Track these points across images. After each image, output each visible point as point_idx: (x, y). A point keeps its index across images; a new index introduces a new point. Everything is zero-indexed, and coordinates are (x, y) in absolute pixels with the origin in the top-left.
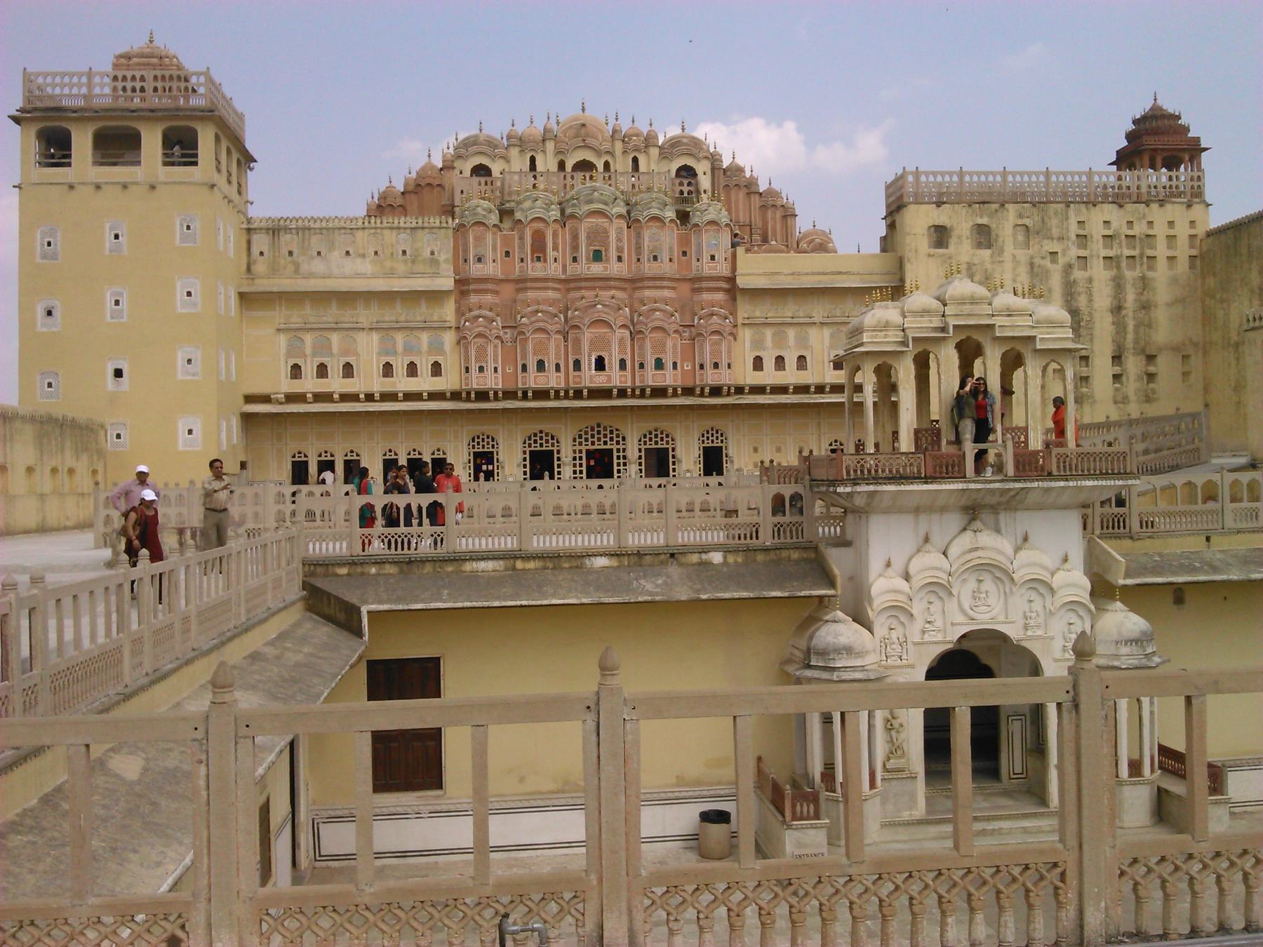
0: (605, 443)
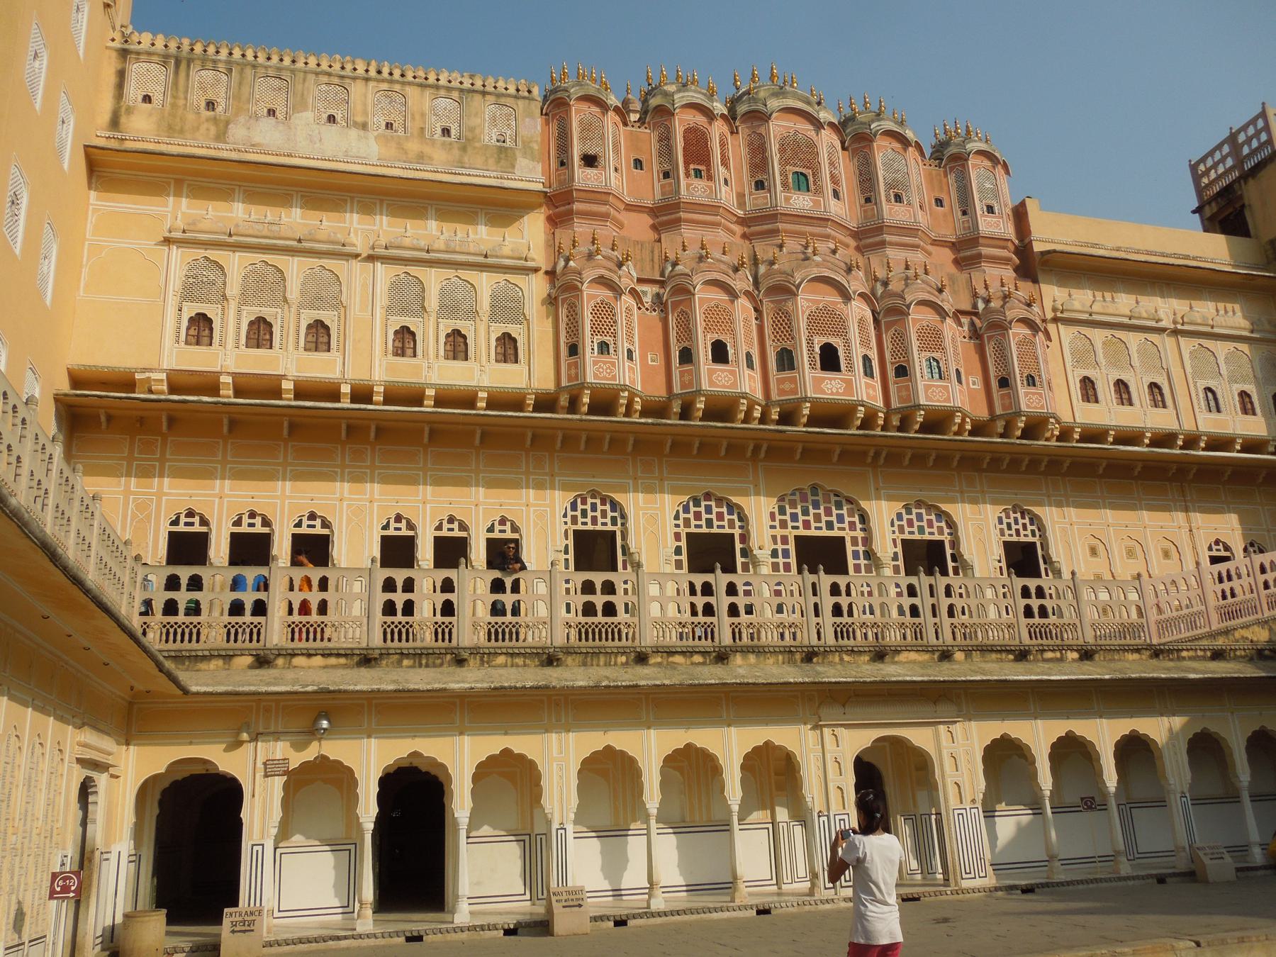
0: (830, 526)
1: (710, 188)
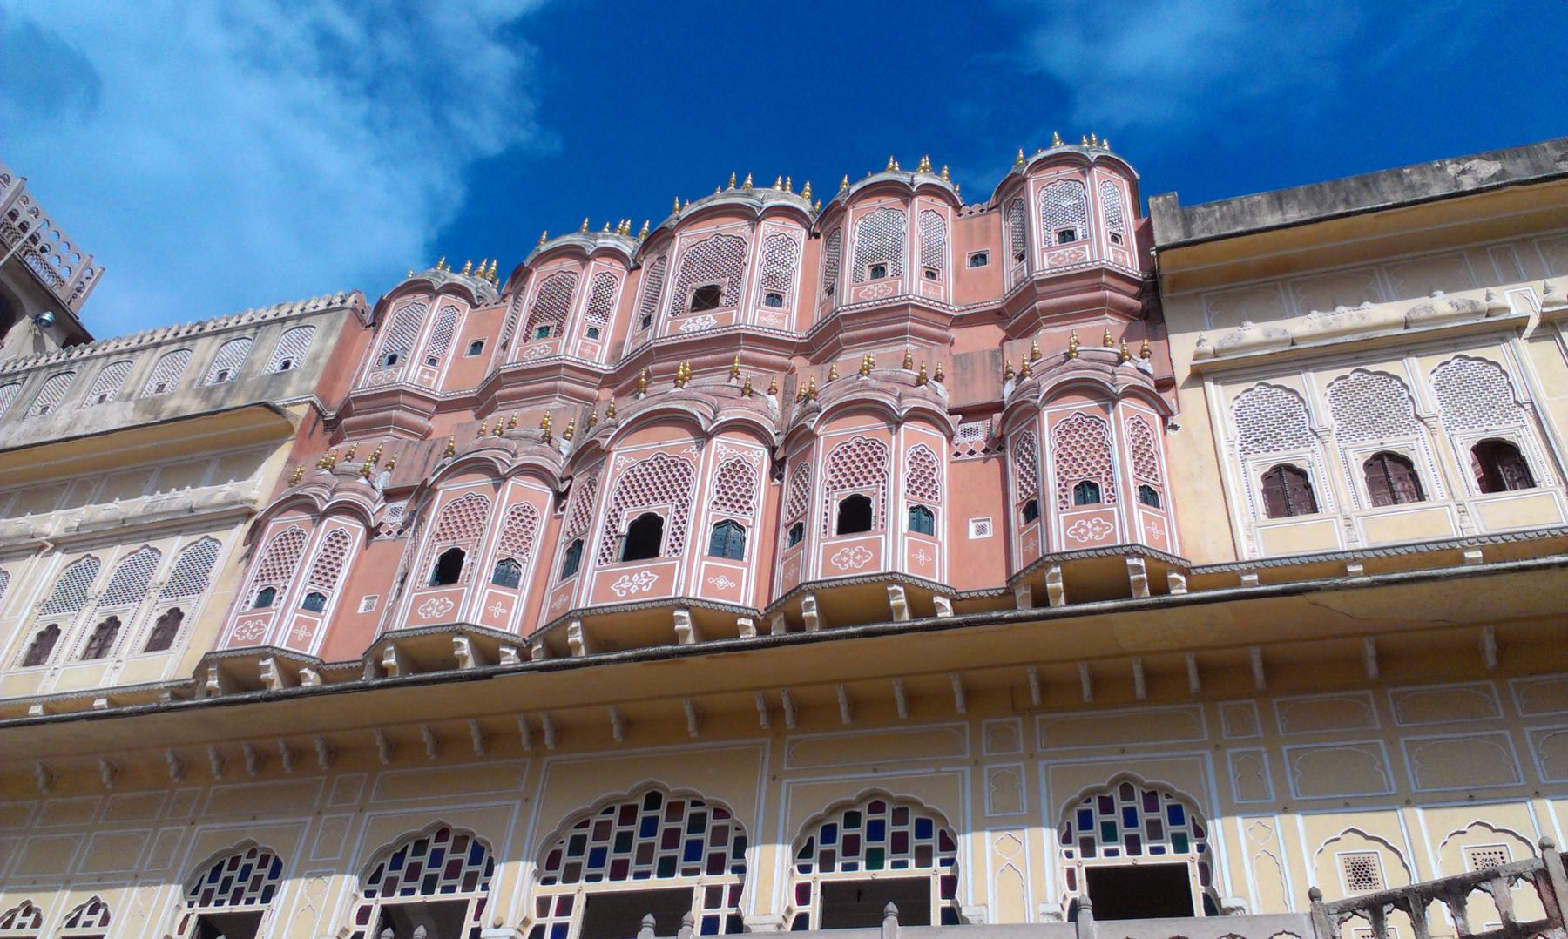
1: (555, 346)
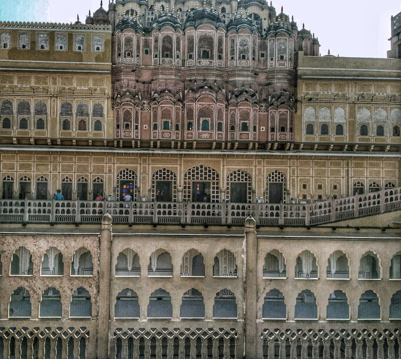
1: (171, 61)
